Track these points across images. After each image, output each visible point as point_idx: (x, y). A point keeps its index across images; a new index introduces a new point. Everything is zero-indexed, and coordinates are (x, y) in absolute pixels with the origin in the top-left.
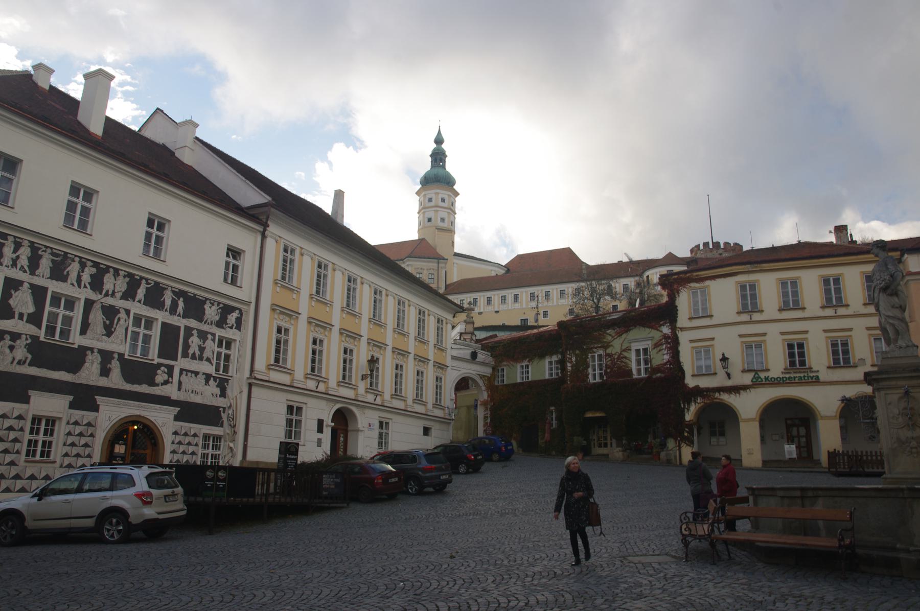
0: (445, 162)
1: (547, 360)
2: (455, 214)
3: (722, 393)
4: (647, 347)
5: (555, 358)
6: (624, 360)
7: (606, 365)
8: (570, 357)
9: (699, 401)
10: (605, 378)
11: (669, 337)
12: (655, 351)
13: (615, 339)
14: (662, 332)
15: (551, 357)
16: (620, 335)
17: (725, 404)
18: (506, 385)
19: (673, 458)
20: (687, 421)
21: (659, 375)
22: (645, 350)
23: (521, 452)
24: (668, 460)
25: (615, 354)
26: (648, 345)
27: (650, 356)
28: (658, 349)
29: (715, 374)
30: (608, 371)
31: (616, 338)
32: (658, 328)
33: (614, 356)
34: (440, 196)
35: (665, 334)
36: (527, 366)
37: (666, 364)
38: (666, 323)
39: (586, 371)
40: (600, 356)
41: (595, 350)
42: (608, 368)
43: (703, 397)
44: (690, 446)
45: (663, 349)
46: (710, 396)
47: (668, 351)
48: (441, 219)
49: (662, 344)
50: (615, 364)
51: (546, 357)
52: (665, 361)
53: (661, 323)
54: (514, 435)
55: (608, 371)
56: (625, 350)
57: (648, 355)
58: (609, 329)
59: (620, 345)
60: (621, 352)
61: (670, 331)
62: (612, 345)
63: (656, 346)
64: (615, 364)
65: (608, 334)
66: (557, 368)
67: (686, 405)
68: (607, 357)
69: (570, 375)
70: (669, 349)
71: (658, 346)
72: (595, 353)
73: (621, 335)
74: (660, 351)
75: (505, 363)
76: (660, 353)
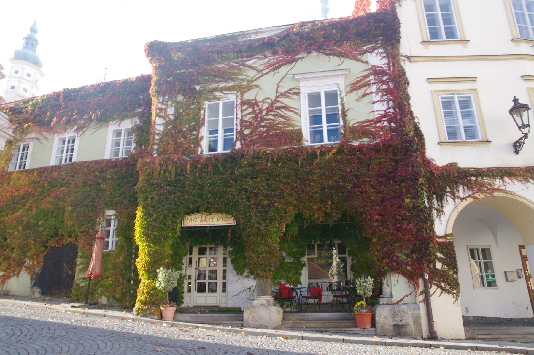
0: (36, 48)
1: (112, 127)
2: (38, 89)
3: (506, 179)
4: (334, 88)
5: (127, 124)
6: (283, 112)
7: (242, 121)
8: (163, 107)
9: (461, 194)
10: (238, 146)
11: (383, 72)
12: (355, 95)
13: (263, 75)
14: (367, 62)
15: (120, 123)
16: (275, 67)
17: (521, 203)
18: (26, 171)
19: (409, 320)
20: (440, 237)
21: (365, 140)
22: (332, 97)
23: (37, 295)
24: (396, 326)
25: (263, 102)
26: (338, 85)
27: (343, 105)
28: (361, 92)
29: (488, 142)
30: (247, 132)
31: (267, 73)
32: (359, 57)
33: (260, 104)
34: (26, 72)
35: (375, 67)
36: (74, 141)
37: (378, 120)
38: (374, 49)
39: (195, 133)
40: (229, 108)
41: (218, 94)
42: (247, 127)
43: (469, 185)
44: (449, 292)
45: (371, 93)
46: (483, 185)
47: (383, 95)
48: (24, 89)
49: (368, 85)
50: (263, 120)
51: (111, 122)
52: (377, 115)
53: (365, 48)
54: (28, 262)
55: (247, 132)
56: (285, 95)
57: (337, 104)
58: (251, 56)
59: (276, 86)
60: (277, 97)
61: (385, 61)
62: (257, 86)
63: (355, 87)
64: (263, 120)
65: (250, 67)
66: (129, 143)
67: (435, 201)
68: (245, 107)
69: (161, 140)
70: (388, 92)
71: (360, 87)
72: (218, 99)
73: (278, 68)
74: (364, 95)
75: (33, 135)
76: (366, 99)
